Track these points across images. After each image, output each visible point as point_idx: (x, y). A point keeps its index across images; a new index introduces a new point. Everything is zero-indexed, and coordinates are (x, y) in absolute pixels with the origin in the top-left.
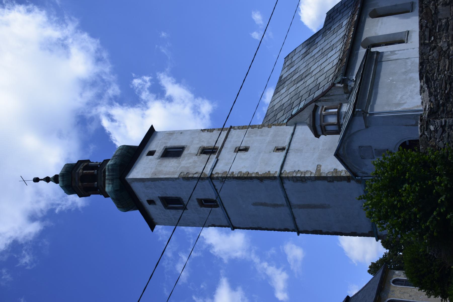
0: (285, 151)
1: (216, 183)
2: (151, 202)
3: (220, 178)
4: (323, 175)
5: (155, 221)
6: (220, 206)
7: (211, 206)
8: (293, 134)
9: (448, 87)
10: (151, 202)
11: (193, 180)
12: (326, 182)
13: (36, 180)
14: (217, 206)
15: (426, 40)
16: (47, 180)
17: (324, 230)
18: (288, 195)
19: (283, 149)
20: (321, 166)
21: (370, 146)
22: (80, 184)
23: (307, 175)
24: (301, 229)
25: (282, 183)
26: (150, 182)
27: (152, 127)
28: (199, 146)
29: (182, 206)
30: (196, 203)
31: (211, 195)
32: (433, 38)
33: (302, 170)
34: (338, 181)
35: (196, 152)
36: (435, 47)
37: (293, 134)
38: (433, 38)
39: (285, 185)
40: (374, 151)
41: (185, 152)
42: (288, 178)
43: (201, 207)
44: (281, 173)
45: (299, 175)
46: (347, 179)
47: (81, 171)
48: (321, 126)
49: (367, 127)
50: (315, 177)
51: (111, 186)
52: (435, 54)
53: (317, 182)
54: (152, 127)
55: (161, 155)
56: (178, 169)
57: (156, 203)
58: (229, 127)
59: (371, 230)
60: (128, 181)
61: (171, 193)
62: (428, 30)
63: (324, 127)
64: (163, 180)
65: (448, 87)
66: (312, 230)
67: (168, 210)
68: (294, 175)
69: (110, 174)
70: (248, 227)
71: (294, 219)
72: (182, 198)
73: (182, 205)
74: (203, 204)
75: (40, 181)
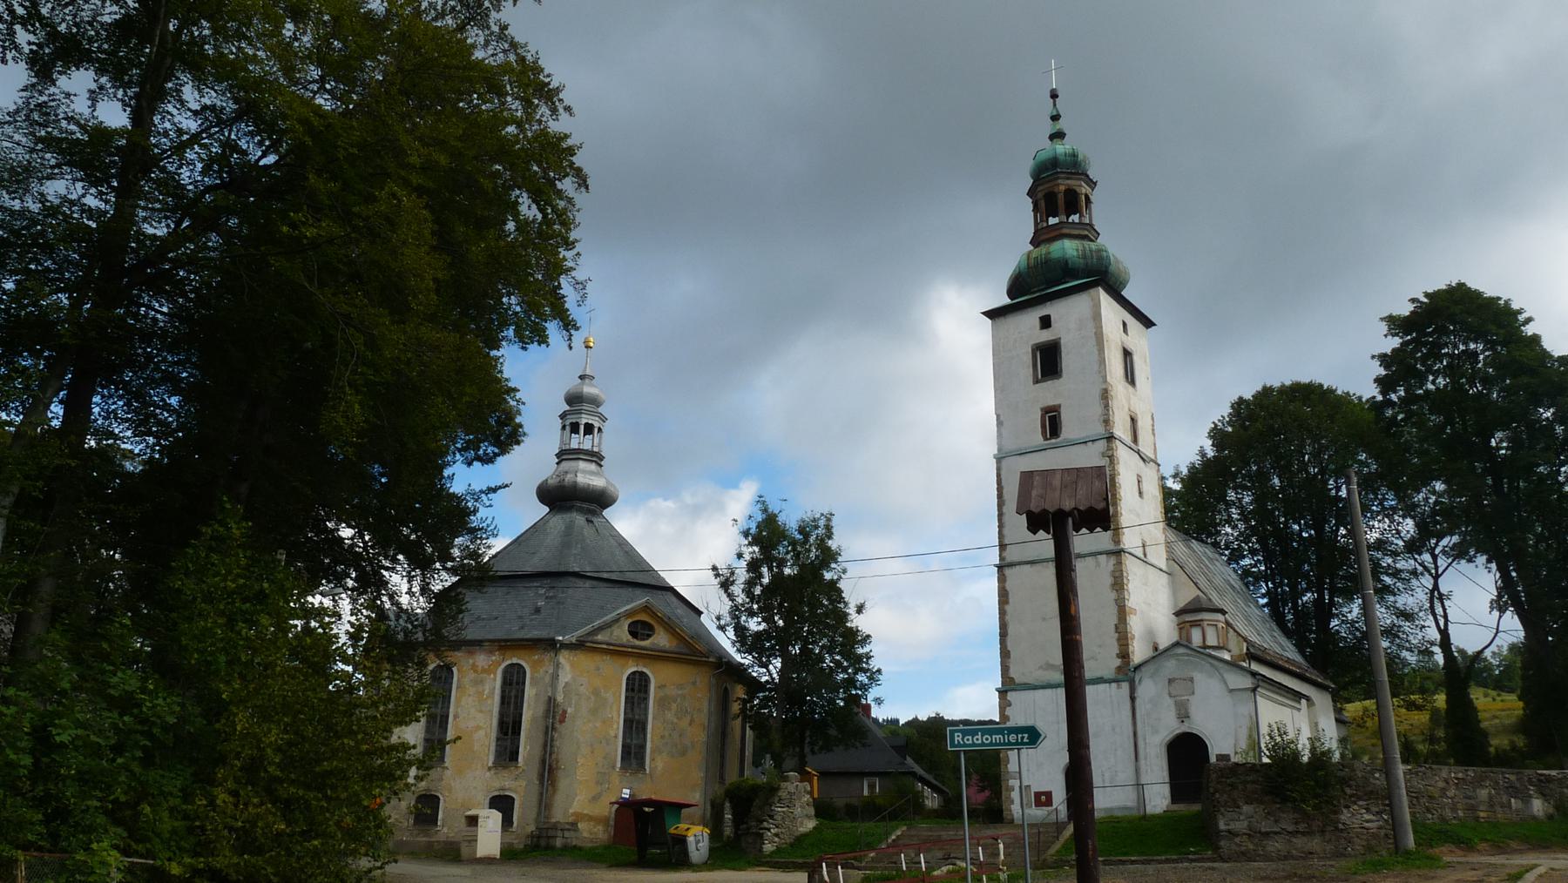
0: (1142, 556)
1: (1102, 445)
2: (1046, 322)
3: (1111, 452)
4: (1128, 618)
5: (1001, 321)
6: (1046, 442)
7: (1043, 426)
8: (1161, 570)
9: (1413, 795)
10: (1046, 322)
11: (1103, 406)
12: (1114, 620)
13: (1054, 95)
14: (1046, 439)
15: (1455, 773)
16: (1055, 118)
17: (1008, 608)
18: (1083, 559)
19: (1145, 555)
20: (1135, 614)
21: (1193, 693)
22: (1062, 188)
23: (1126, 593)
24: (1008, 572)
25: (1109, 553)
26: (1094, 330)
27: (1155, 325)
28: (1138, 413)
29: (1040, 376)
30: (1051, 403)
31: (1069, 431)
32: (1456, 781)
33: (1130, 585)
34: (1119, 640)
35: (1132, 409)
36: (1448, 783)
37: (1161, 570)
38: (1456, 781)
39: (1103, 558)
40: (1186, 698)
41: (1130, 387)
42: (1120, 563)
43: (1042, 409)
44: (1124, 552)
45: (1125, 581)
46: (1124, 655)
47: (1084, 191)
48: (1202, 620)
49: (1231, 691)
50: (1124, 606)
51: (1075, 254)
52: (1441, 784)
53: (1113, 610)
54: (1155, 325)
55: (1126, 347)
56: (1114, 380)
57: (1045, 330)
58: (1159, 462)
59: (1017, 681)
60: (1092, 291)
61: (1068, 361)
62: (1465, 777)
63: (1200, 625)
64: (1099, 354)
65: (1413, 795)
66: (1008, 588)
67: (1030, 350)
68: (1125, 574)
69: (1094, 254)
70: (1004, 483)
71: (1032, 563)
72: (1061, 380)
73: (1042, 376)
74: (1047, 413)
75: (1052, 100)
